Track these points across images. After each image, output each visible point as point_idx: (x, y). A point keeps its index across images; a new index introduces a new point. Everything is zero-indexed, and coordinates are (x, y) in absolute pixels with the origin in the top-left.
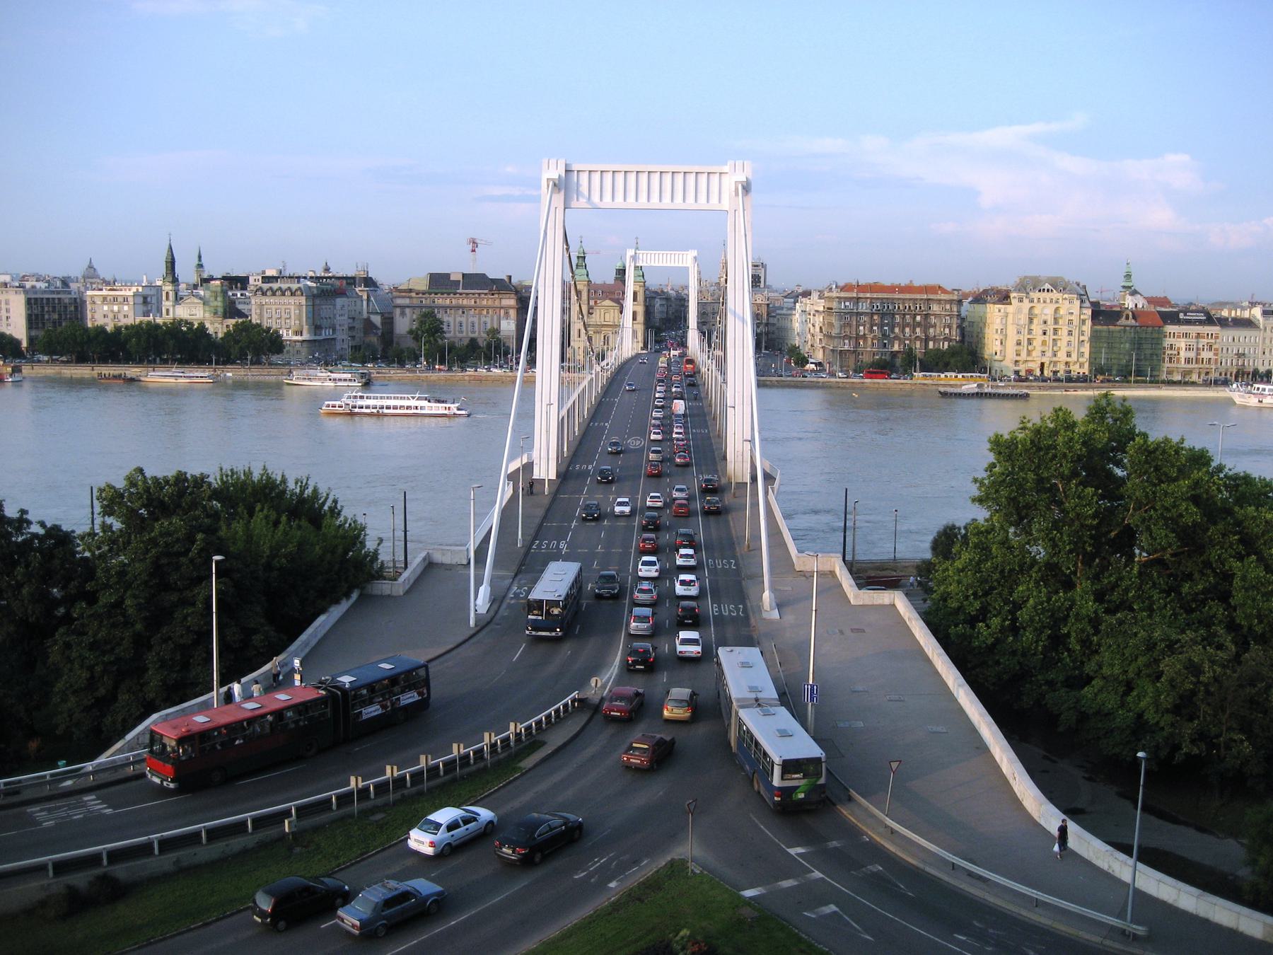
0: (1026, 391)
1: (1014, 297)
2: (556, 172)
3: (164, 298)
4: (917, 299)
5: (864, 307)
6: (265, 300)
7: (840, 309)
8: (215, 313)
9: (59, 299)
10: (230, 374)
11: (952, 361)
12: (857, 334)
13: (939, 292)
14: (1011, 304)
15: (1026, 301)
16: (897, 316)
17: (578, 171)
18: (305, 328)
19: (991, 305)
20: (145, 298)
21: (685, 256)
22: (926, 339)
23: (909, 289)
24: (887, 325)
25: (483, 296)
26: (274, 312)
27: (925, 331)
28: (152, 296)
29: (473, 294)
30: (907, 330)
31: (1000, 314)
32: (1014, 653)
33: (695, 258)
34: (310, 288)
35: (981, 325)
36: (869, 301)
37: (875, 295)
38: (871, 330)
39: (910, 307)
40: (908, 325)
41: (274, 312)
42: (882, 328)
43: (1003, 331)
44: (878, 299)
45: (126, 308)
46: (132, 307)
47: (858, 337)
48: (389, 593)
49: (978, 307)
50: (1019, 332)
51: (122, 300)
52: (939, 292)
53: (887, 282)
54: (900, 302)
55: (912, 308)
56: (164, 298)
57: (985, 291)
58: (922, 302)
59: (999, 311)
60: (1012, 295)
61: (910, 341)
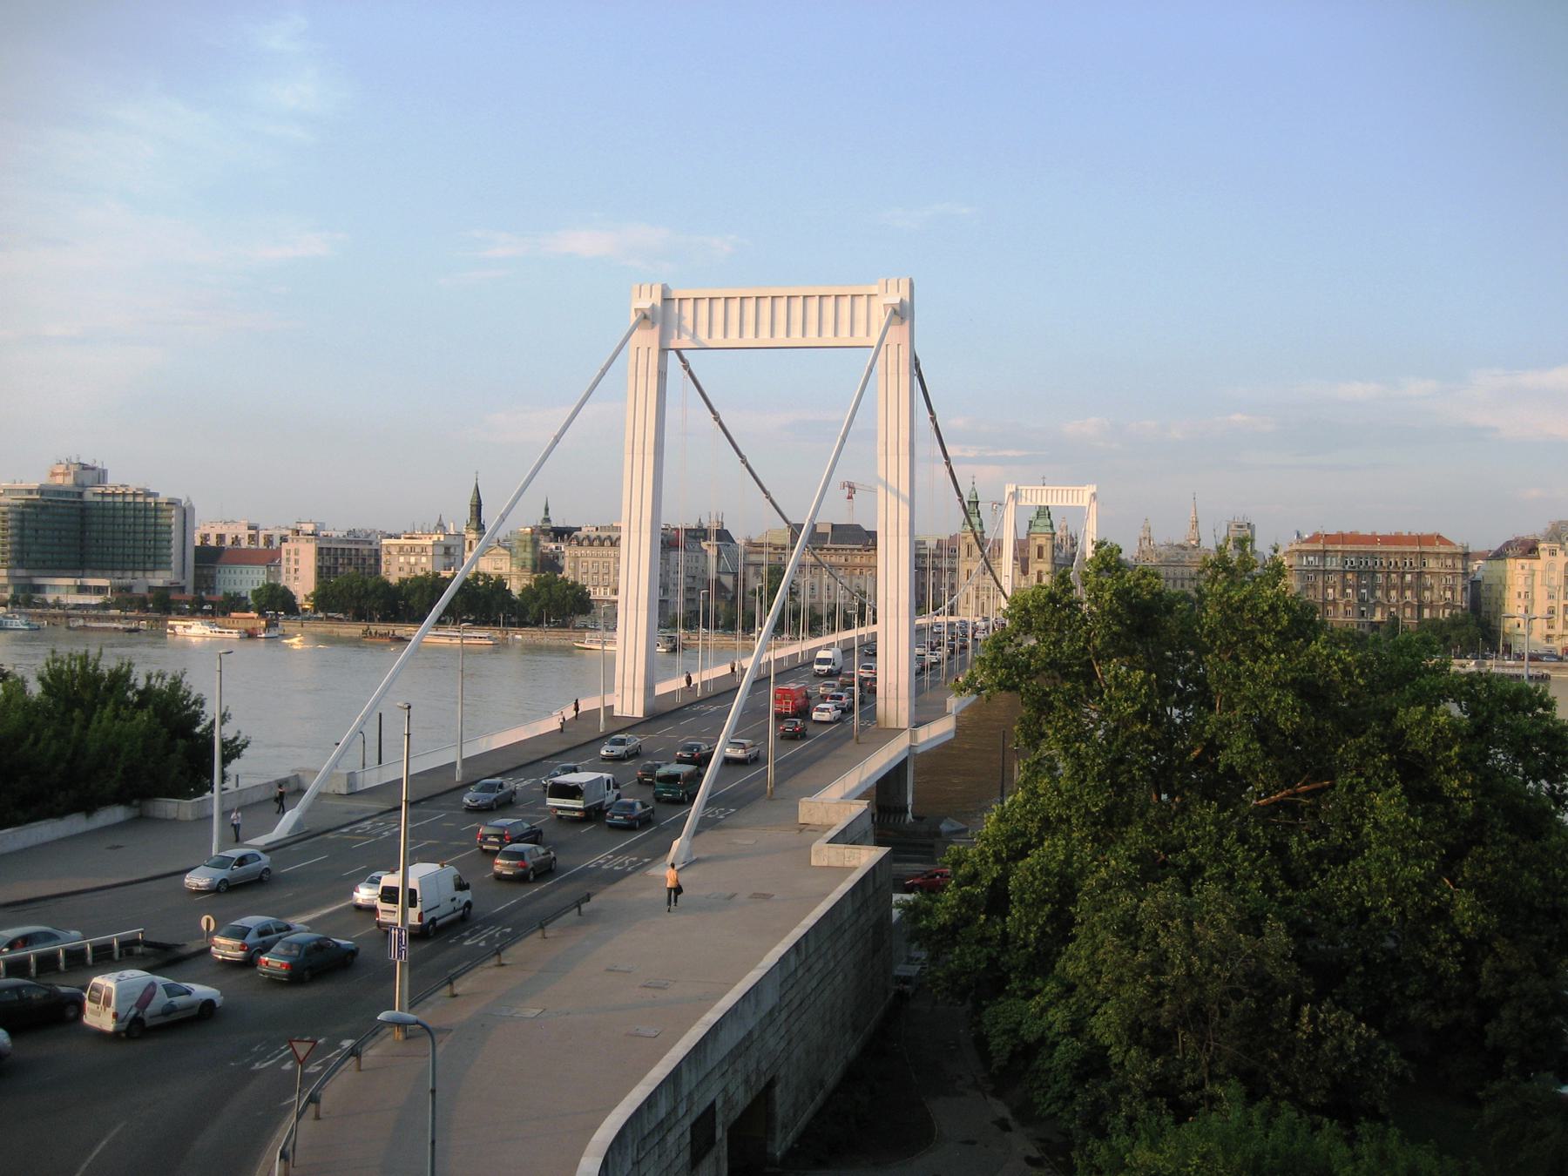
0: (1545, 671)
1: (1544, 549)
2: (648, 300)
3: (467, 548)
4: (1406, 553)
5: (1333, 563)
6: (581, 551)
7: (1301, 565)
8: (524, 567)
9: (357, 550)
10: (519, 637)
11: (1453, 634)
12: (1325, 599)
13: (1437, 543)
14: (1538, 558)
15: (1560, 554)
16: (1379, 575)
17: (680, 299)
19: (1512, 561)
20: (447, 549)
21: (1080, 492)
22: (1419, 606)
23: (1396, 539)
24: (1365, 586)
25: (856, 552)
26: (590, 566)
27: (1418, 596)
28: (455, 546)
29: (843, 549)
30: (1393, 593)
31: (1524, 572)
32: (983, 941)
33: (1094, 495)
35: (1501, 587)
36: (1340, 554)
37: (1348, 548)
38: (1344, 594)
39: (1396, 563)
40: (1394, 587)
41: (590, 566)
42: (1358, 590)
43: (1528, 595)
44: (1352, 552)
45: (424, 560)
46: (430, 558)
48: (175, 815)
49: (1496, 565)
50: (1551, 597)
51: (420, 550)
52: (1437, 543)
53: (1365, 530)
54: (1382, 556)
55: (1399, 564)
56: (467, 548)
57: (1508, 545)
58: (1413, 556)
59: (1523, 568)
60: (1541, 546)
61: (1397, 607)
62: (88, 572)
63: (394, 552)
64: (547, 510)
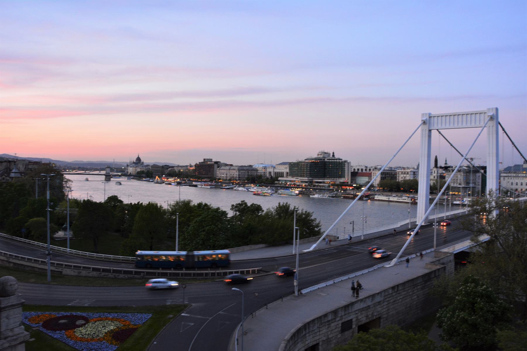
18: (462, 183)
28: (416, 172)
34: (465, 169)
45: (408, 175)
62: (326, 178)
63: (400, 173)
64: (446, 161)
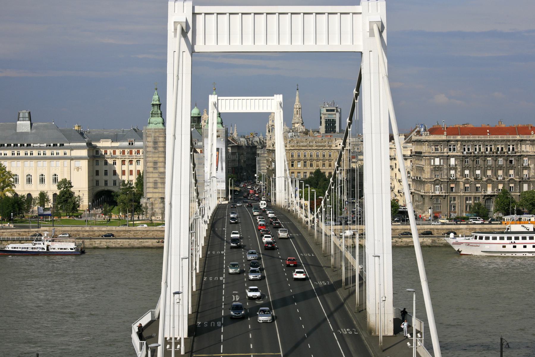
30: (500, 173)
37: (466, 138)
40: (501, 167)
47: (450, 181)
54: (492, 143)
55: (504, 150)
